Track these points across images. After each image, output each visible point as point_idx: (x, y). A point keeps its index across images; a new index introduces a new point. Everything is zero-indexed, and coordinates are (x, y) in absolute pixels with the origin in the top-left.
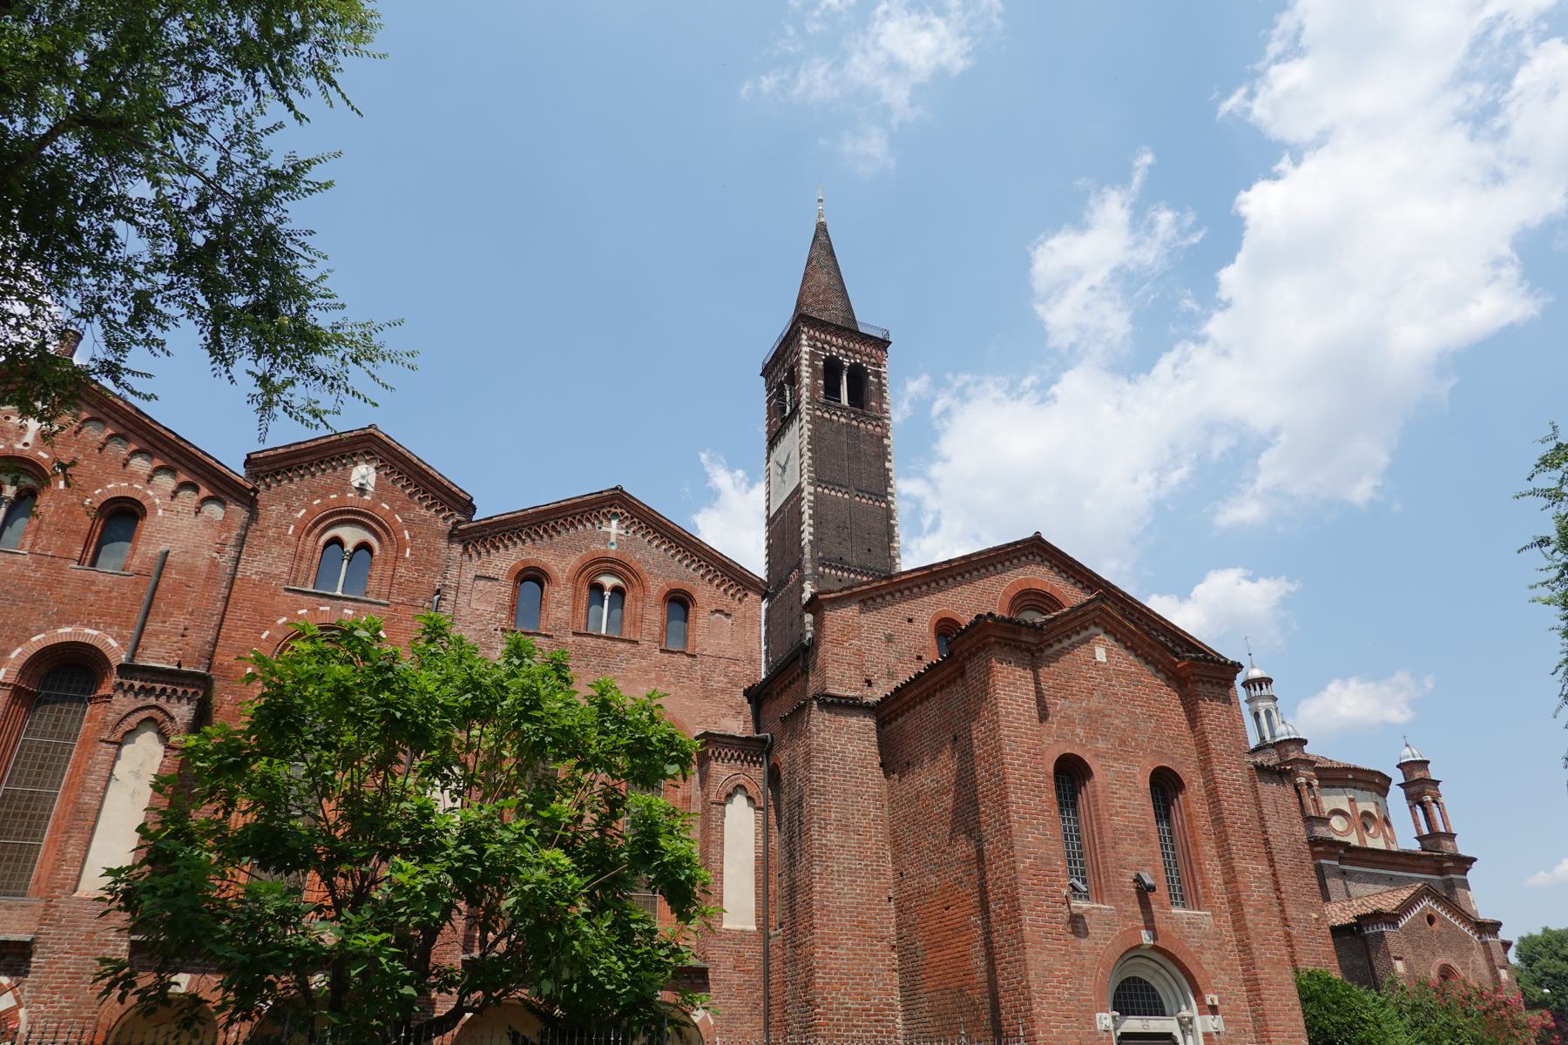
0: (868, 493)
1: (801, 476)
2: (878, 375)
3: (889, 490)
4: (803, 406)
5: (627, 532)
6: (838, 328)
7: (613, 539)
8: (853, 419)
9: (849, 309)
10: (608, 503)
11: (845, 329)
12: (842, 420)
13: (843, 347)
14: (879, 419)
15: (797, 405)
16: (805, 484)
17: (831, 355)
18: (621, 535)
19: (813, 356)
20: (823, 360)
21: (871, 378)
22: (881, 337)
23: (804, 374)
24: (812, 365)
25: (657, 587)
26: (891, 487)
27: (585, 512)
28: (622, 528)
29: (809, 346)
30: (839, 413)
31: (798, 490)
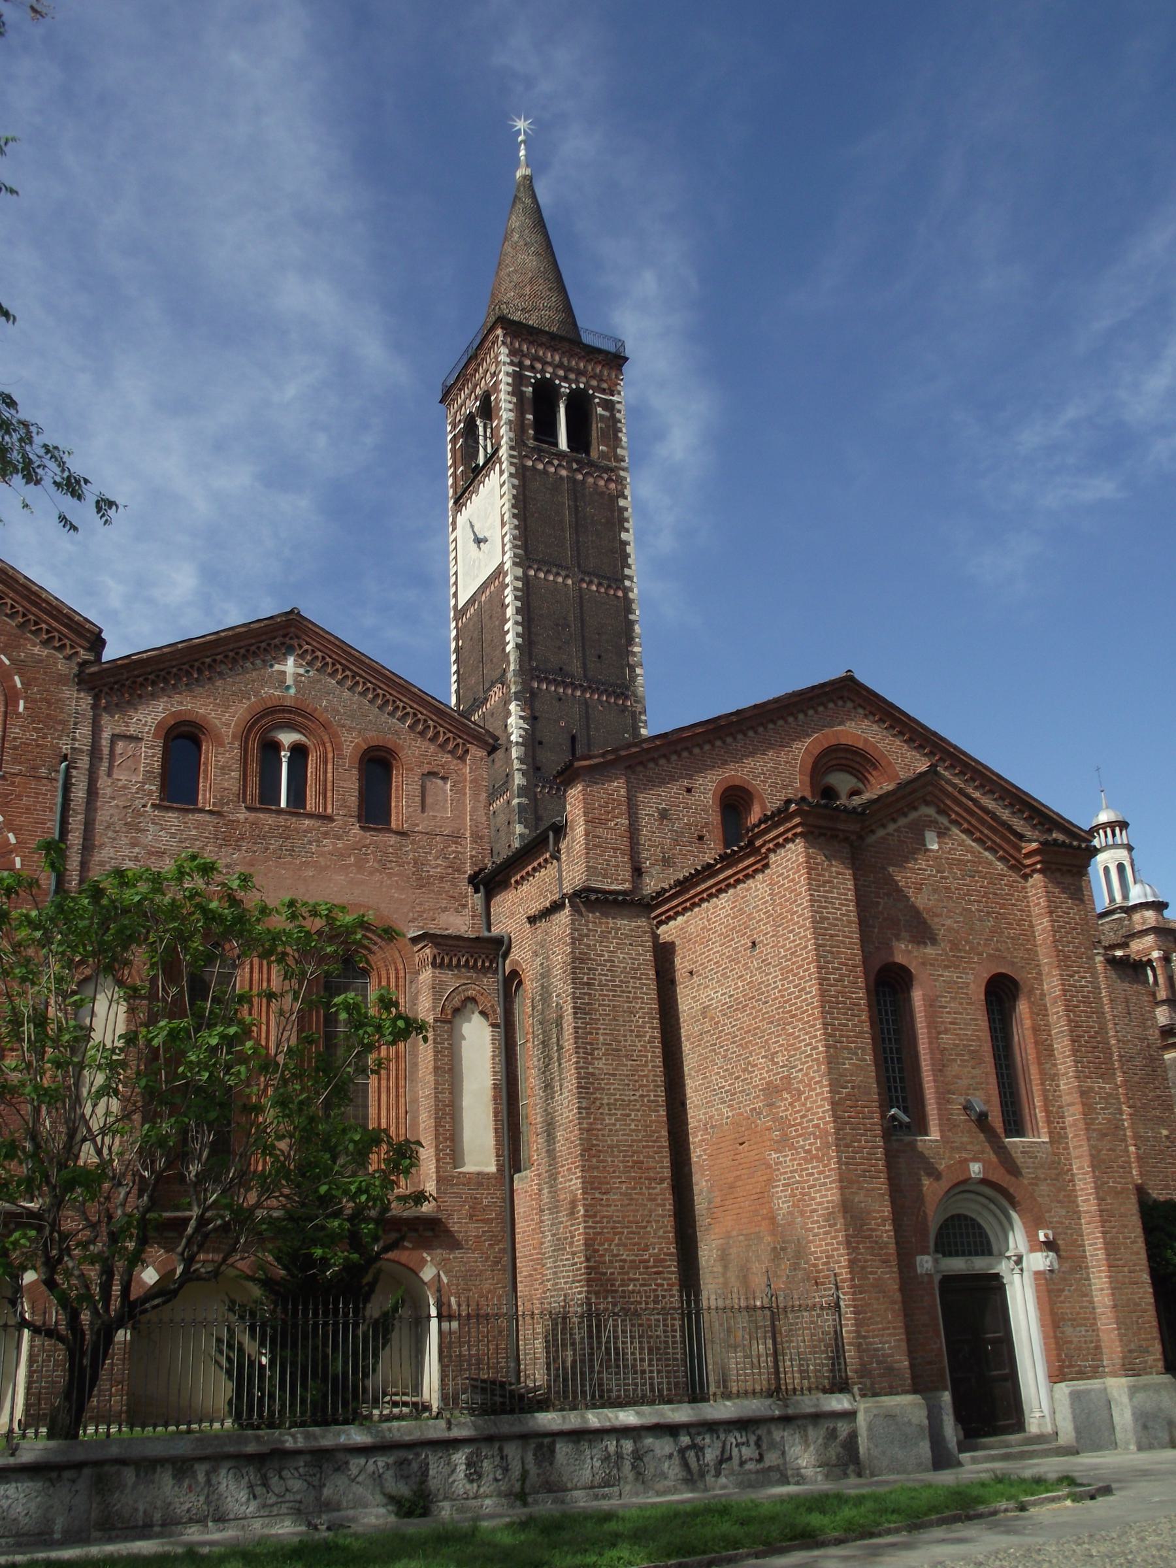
0: (597, 576)
1: (504, 553)
2: (609, 406)
3: (627, 571)
4: (503, 452)
5: (308, 671)
6: (552, 336)
7: (289, 681)
8: (576, 470)
9: (568, 309)
10: (281, 633)
11: (562, 339)
12: (564, 473)
13: (560, 365)
14: (612, 470)
15: (496, 451)
16: (507, 566)
17: (544, 377)
18: (301, 675)
19: (518, 379)
20: (533, 385)
21: (599, 410)
22: (613, 349)
23: (503, 405)
24: (516, 392)
25: (351, 743)
26: (629, 567)
27: (252, 645)
28: (301, 666)
29: (512, 363)
30: (556, 462)
31: (499, 572)
